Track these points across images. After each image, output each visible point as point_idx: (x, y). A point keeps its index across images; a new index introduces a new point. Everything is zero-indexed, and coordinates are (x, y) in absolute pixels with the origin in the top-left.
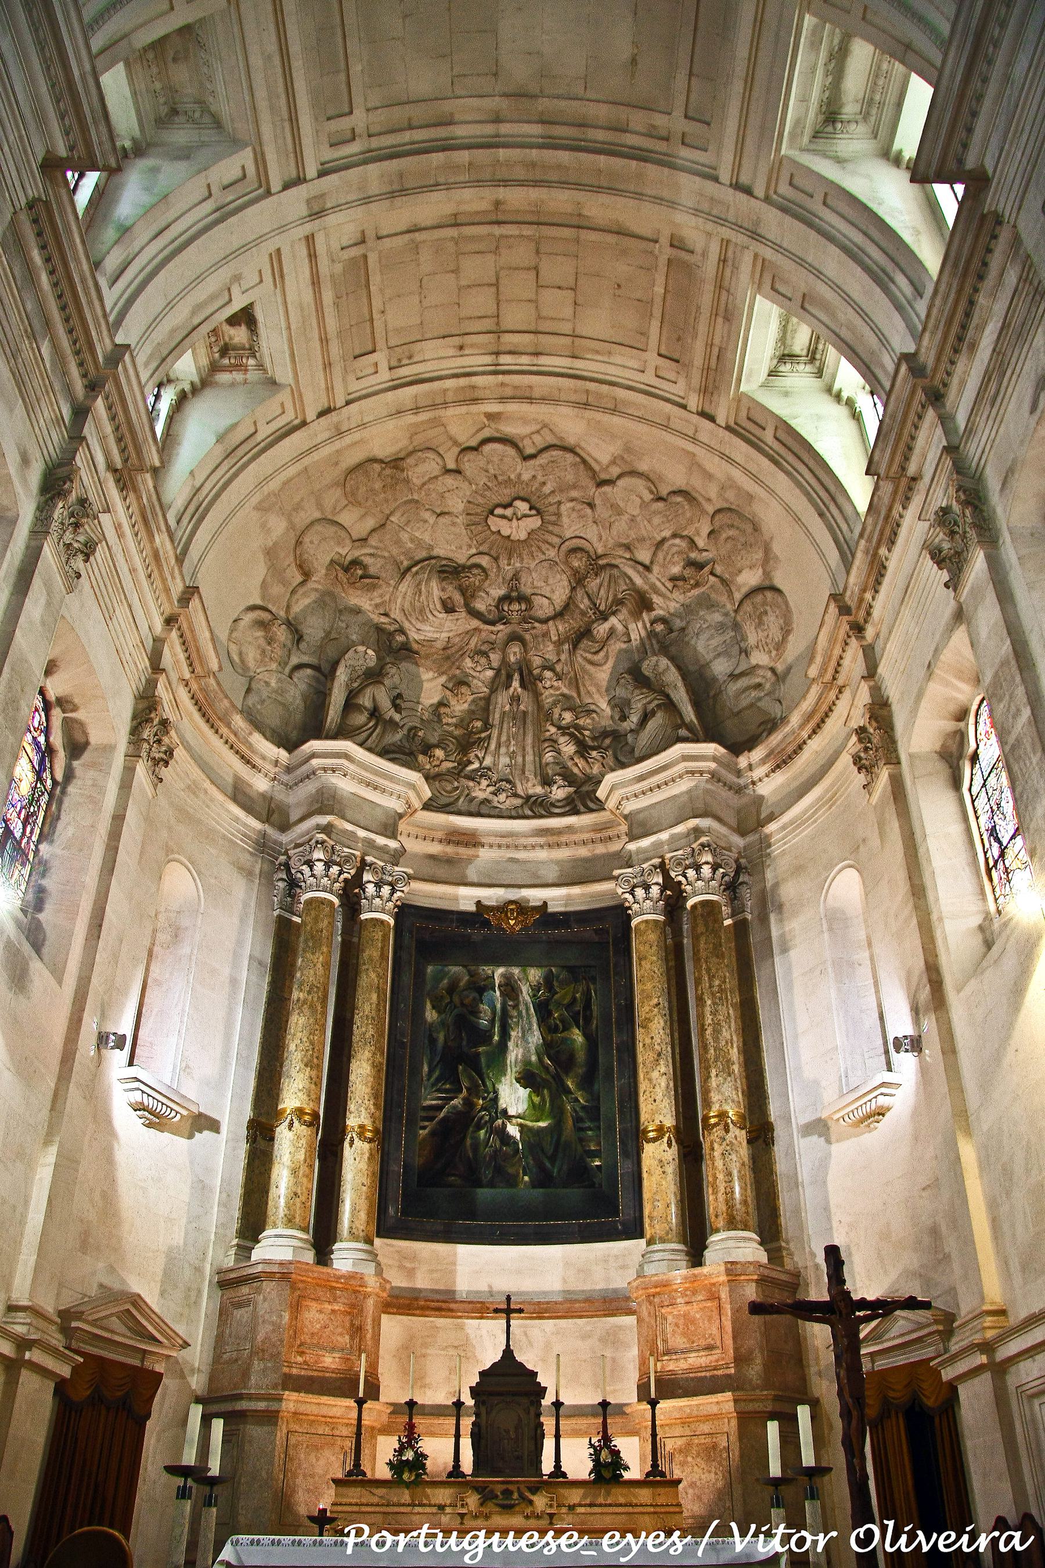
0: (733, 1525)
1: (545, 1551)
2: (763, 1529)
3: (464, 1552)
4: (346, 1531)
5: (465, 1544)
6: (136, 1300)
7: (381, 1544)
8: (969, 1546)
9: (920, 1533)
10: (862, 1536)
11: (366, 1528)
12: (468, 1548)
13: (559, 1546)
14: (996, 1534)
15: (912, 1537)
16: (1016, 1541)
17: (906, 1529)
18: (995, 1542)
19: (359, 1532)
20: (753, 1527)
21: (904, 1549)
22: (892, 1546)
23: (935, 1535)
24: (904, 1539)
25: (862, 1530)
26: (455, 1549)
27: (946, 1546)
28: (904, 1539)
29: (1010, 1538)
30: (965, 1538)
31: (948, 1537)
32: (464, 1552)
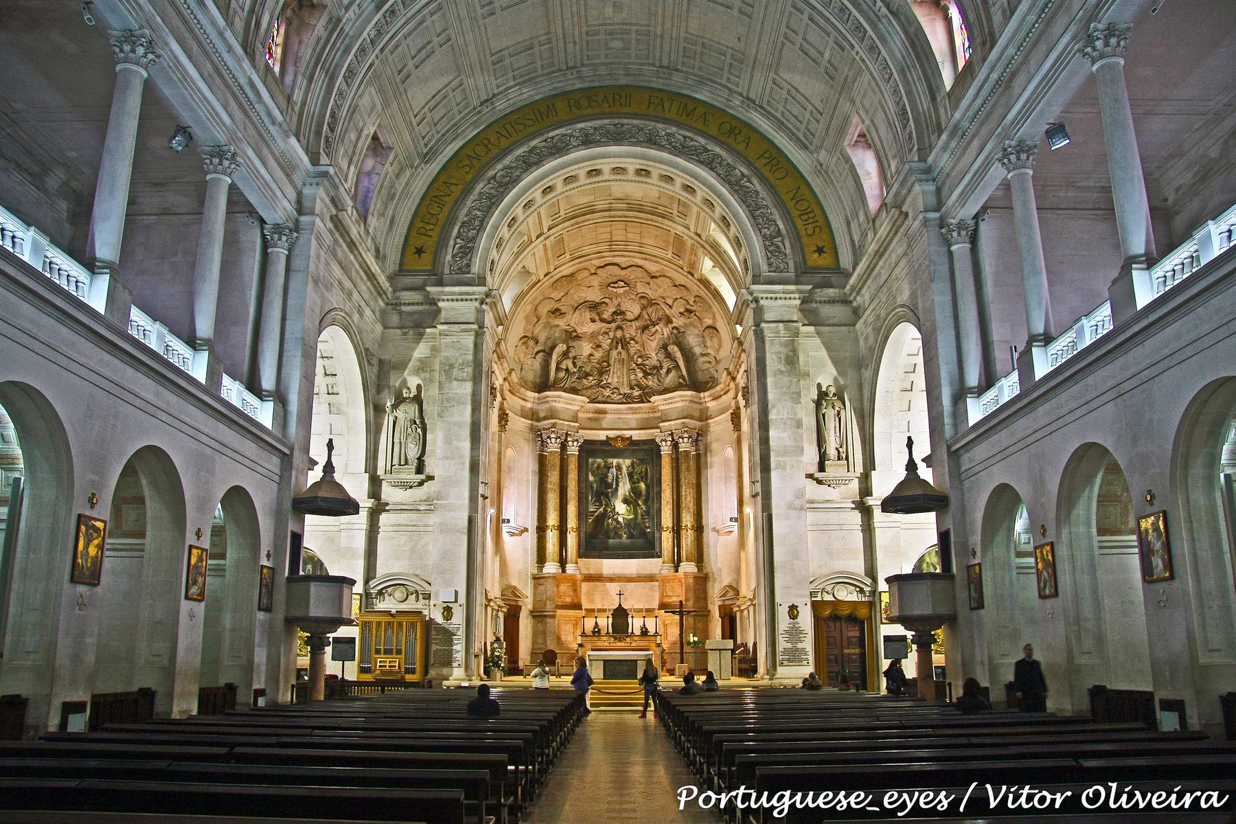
1: (838, 808)
2: (1012, 790)
4: (679, 791)
5: (774, 802)
6: (515, 588)
8: (1176, 804)
9: (1137, 793)
10: (1091, 795)
11: (695, 790)
12: (776, 805)
13: (849, 803)
14: (1198, 793)
15: (1131, 796)
16: (1214, 800)
17: (1126, 790)
18: (1196, 801)
19: (690, 792)
20: (1004, 788)
21: (1125, 806)
23: (1149, 795)
24: (1124, 797)
25: (1091, 791)
28: (1124, 797)
29: (1209, 797)
30: (1174, 797)
31: (1160, 796)
32: (773, 808)
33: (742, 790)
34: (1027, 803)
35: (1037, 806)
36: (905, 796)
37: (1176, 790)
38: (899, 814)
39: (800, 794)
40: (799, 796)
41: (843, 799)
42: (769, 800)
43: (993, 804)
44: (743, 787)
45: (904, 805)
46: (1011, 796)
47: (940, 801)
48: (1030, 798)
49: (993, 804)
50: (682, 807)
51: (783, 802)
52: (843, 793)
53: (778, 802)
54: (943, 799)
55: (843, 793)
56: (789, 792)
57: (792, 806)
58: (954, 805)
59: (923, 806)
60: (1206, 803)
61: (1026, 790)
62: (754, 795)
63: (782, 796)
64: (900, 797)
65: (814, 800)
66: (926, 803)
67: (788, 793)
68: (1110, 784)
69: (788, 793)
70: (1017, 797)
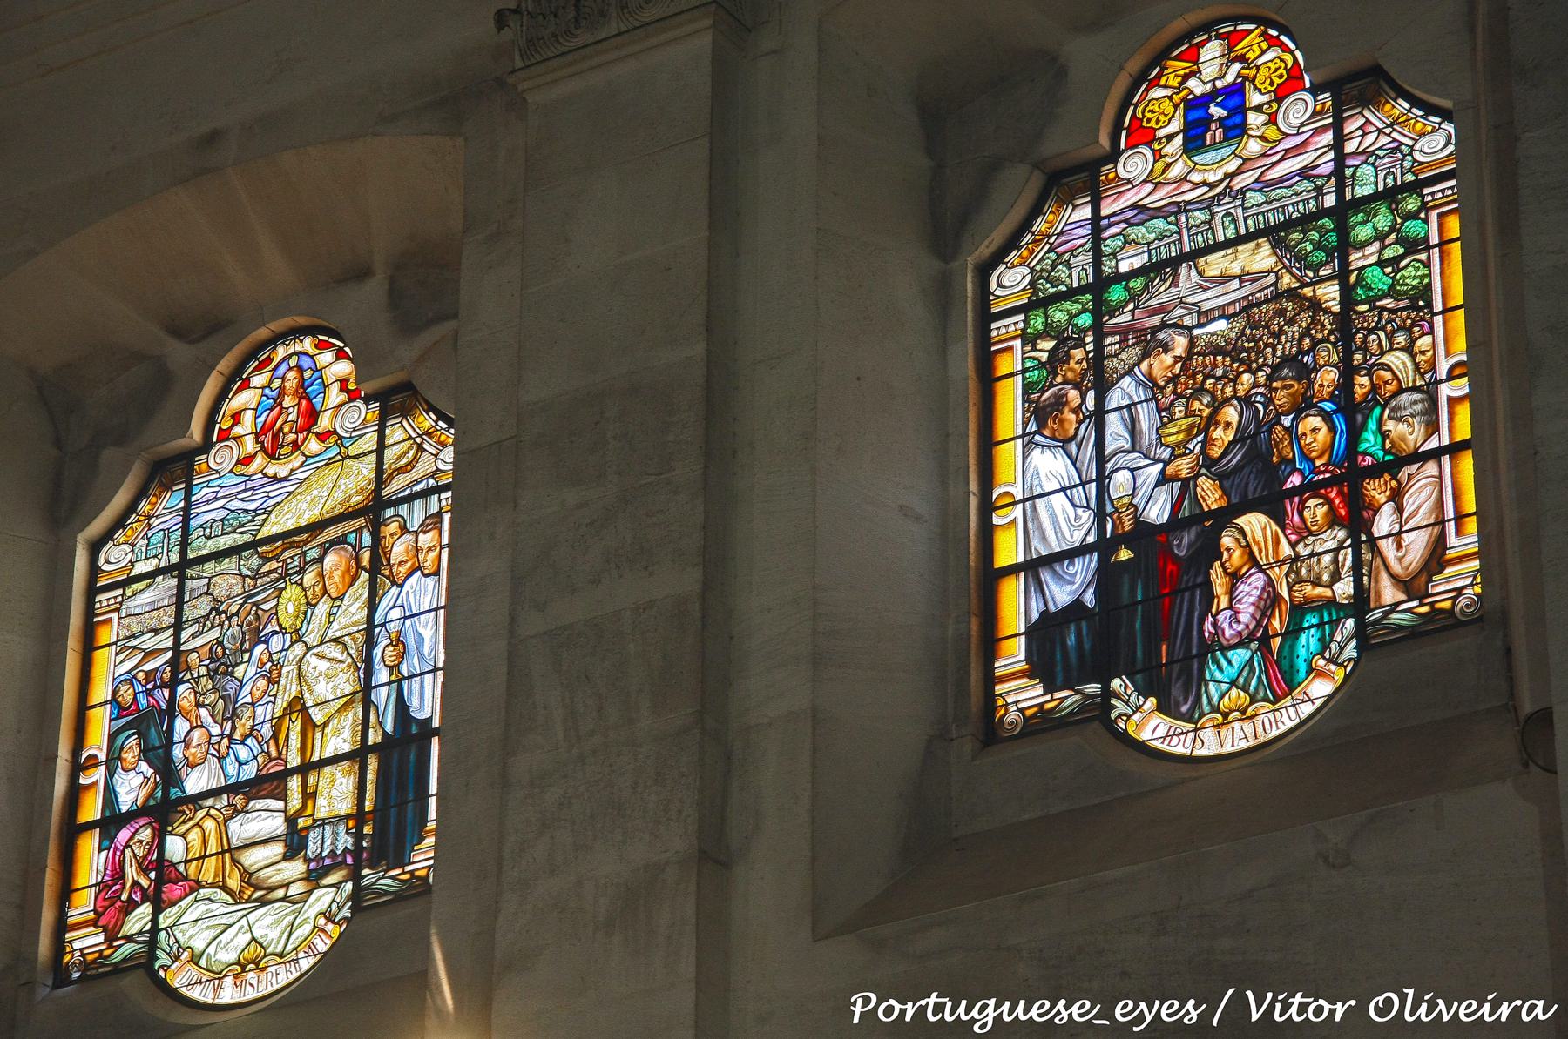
0: (1249, 994)
1: (1057, 1021)
2: (1280, 998)
3: (974, 1021)
4: (852, 1000)
5: (975, 1013)
7: (889, 1011)
8: (1490, 1016)
9: (1440, 1001)
10: (1381, 1005)
13: (1070, 1015)
14: (1519, 1002)
15: (1432, 1006)
16: (1539, 1010)
17: (1427, 998)
19: (867, 1001)
20: (1270, 995)
21: (1424, 1018)
22: (1411, 1015)
23: (1456, 1004)
24: (1424, 1007)
25: (1381, 999)
26: (964, 1018)
27: (1467, 1015)
28: (1424, 1007)
29: (1533, 1007)
30: (1487, 1007)
31: (1469, 1006)
32: (974, 1021)
33: (933, 998)
34: (1299, 1014)
35: (1312, 1018)
36: (1143, 1006)
37: (1490, 998)
38: (1136, 1029)
39: (1007, 1004)
40: (1007, 1005)
41: (1063, 1010)
42: (968, 1011)
43: (1255, 1017)
44: (935, 994)
45: (1141, 1017)
46: (1278, 1006)
47: (1188, 1013)
48: (1303, 1008)
49: (1255, 1017)
50: (856, 1020)
51: (987, 1014)
52: (1063, 1002)
53: (980, 1013)
54: (1192, 1010)
55: (1063, 1002)
56: (993, 1000)
57: (998, 1018)
58: (1205, 1018)
59: (1165, 1018)
60: (1528, 1015)
61: (1298, 999)
62: (949, 1005)
63: (985, 1007)
64: (1136, 1006)
65: (1026, 1011)
66: (1169, 1015)
67: (992, 1002)
68: (1405, 990)
69: (992, 1002)
70: (1286, 1006)
